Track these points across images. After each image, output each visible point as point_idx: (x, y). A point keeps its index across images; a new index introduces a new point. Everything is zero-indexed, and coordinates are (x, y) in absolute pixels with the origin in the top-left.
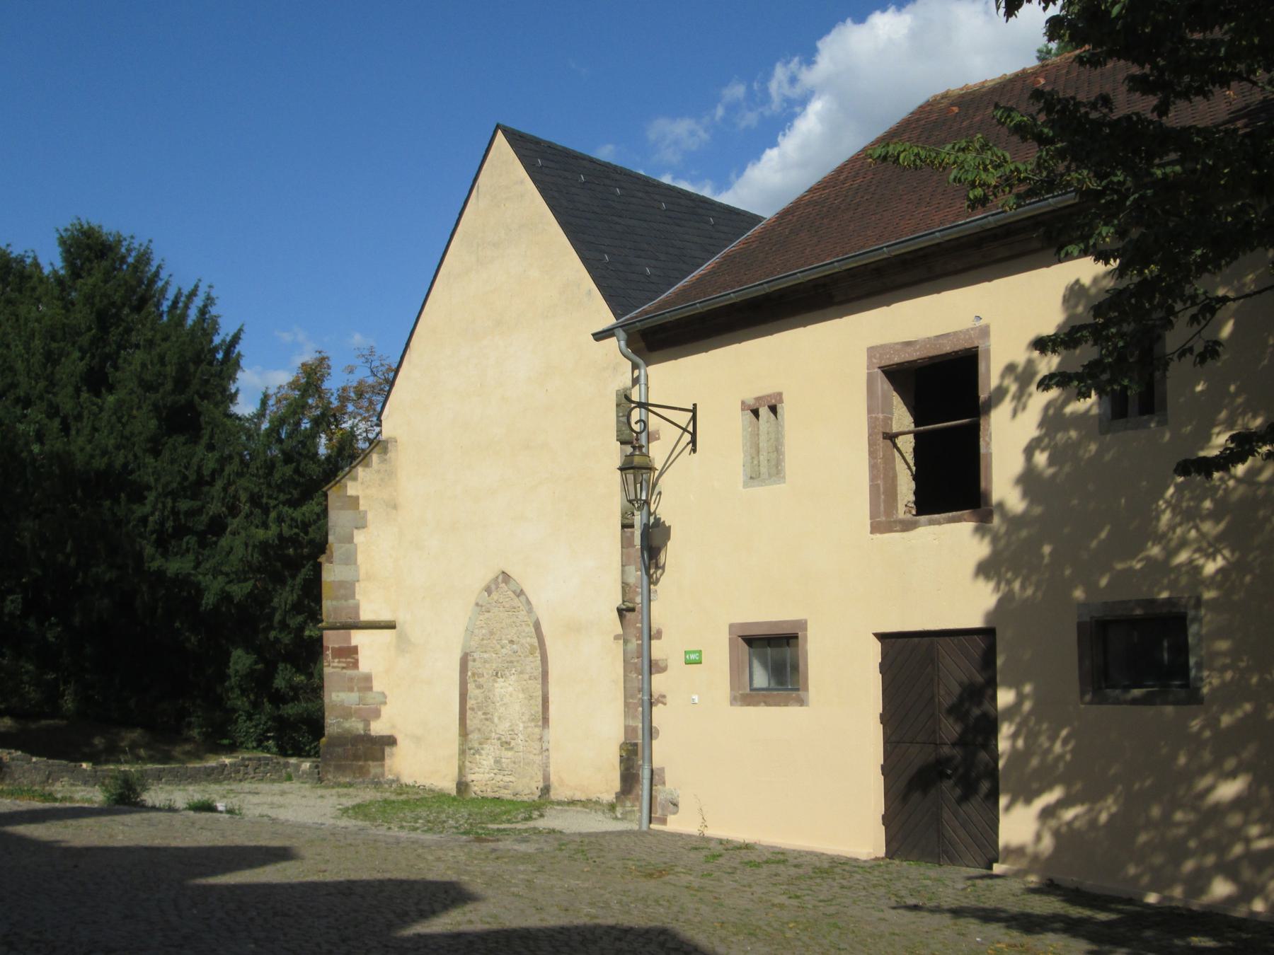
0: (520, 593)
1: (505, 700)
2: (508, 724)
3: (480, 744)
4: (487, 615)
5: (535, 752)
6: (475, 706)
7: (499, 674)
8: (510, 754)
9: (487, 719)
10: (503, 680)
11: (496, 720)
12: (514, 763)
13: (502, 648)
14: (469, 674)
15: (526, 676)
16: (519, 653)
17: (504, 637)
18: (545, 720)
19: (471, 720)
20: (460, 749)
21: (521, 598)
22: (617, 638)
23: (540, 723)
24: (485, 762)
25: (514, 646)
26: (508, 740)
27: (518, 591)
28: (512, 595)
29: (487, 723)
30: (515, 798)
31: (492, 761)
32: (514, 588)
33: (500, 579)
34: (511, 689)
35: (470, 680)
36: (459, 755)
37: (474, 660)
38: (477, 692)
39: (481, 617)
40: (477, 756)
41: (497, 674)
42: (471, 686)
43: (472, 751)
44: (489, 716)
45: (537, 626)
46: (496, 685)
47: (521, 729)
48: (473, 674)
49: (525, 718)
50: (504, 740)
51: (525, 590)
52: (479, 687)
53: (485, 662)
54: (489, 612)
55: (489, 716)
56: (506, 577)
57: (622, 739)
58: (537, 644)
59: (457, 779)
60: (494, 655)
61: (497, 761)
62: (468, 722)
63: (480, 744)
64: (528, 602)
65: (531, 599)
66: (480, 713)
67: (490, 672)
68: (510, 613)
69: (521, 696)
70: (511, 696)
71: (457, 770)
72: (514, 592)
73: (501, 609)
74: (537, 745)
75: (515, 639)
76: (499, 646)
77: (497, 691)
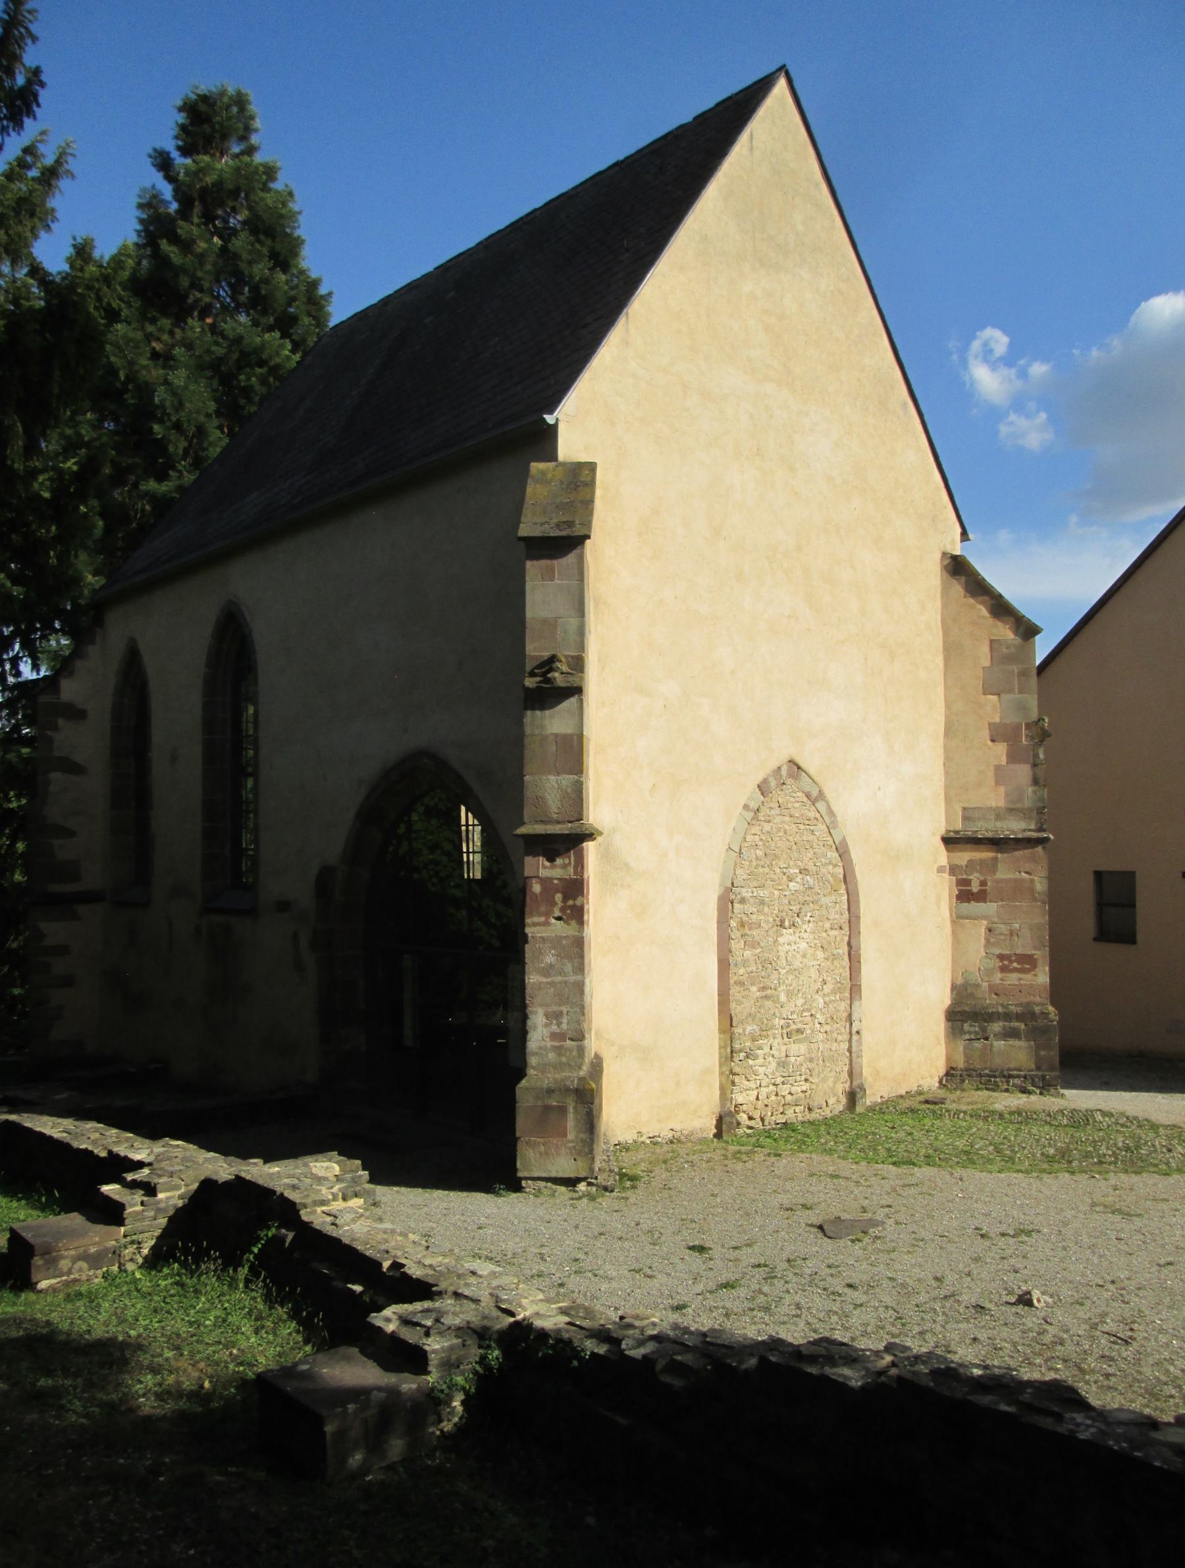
0: (816, 798)
1: (797, 964)
2: (800, 1002)
3: (754, 1040)
4: (767, 827)
5: (840, 1038)
6: (744, 978)
7: (787, 924)
8: (802, 1048)
9: (767, 997)
10: (791, 931)
11: (783, 998)
12: (811, 1060)
13: (791, 881)
14: (733, 923)
15: (827, 925)
16: (817, 889)
17: (792, 863)
18: (855, 990)
19: (739, 1003)
20: (720, 1057)
21: (821, 805)
22: (941, 870)
23: (847, 994)
24: (761, 1070)
25: (808, 877)
26: (800, 1026)
27: (815, 794)
28: (805, 799)
29: (768, 1004)
30: (809, 1117)
31: (774, 1065)
32: (807, 789)
33: (784, 772)
34: (803, 945)
35: (735, 934)
36: (721, 1065)
37: (743, 901)
38: (748, 953)
39: (756, 830)
40: (751, 1062)
41: (782, 925)
42: (736, 945)
43: (742, 1055)
44: (769, 992)
45: (843, 851)
46: (781, 940)
47: (821, 1005)
48: (742, 924)
49: (827, 989)
50: (794, 1027)
51: (827, 792)
52: (754, 945)
53: (762, 903)
54: (769, 821)
55: (769, 992)
56: (795, 767)
57: (947, 1002)
58: (842, 876)
59: (717, 1110)
60: (776, 893)
61: (782, 1064)
62: (733, 1005)
63: (754, 1040)
64: (831, 813)
65: (835, 809)
66: (754, 989)
67: (771, 919)
68: (802, 827)
69: (820, 955)
70: (804, 956)
71: (717, 1092)
72: (808, 796)
73: (787, 818)
74: (843, 1027)
75: (810, 866)
76: (785, 878)
77: (783, 950)
